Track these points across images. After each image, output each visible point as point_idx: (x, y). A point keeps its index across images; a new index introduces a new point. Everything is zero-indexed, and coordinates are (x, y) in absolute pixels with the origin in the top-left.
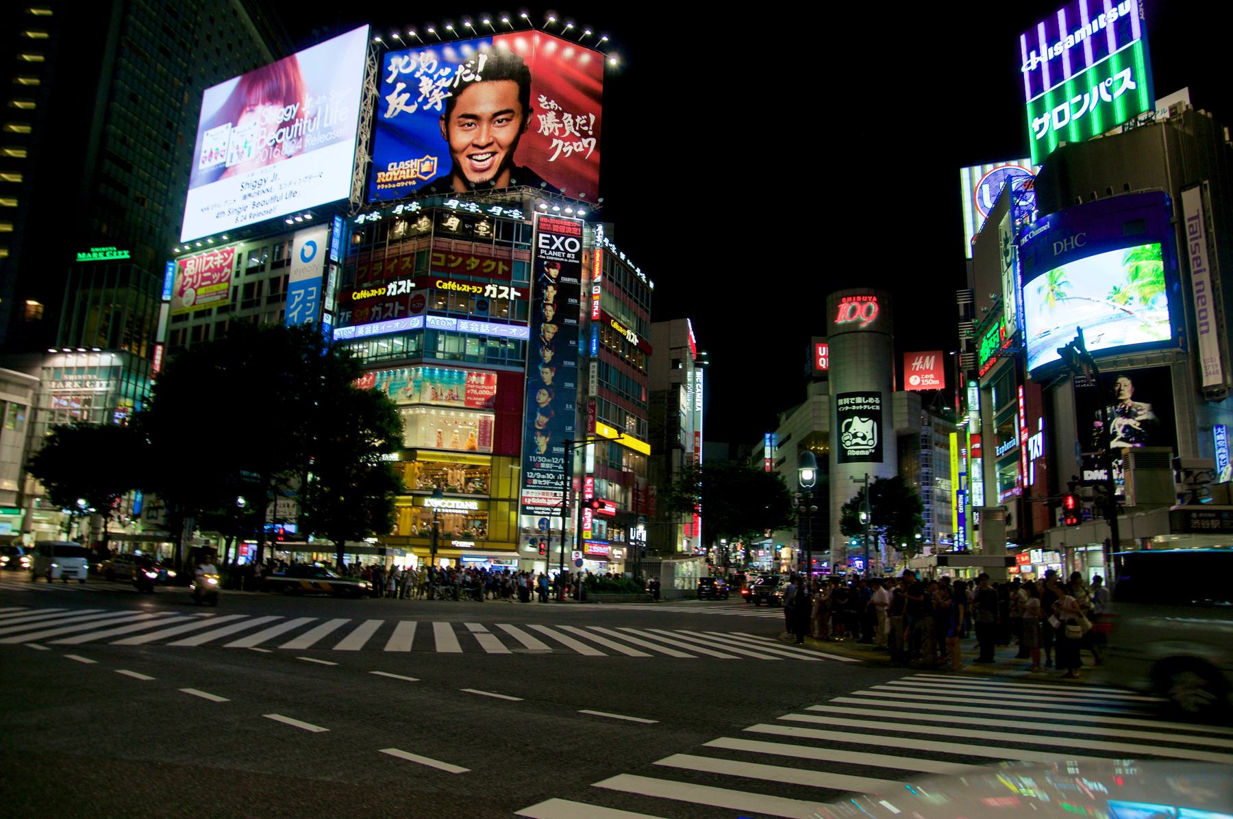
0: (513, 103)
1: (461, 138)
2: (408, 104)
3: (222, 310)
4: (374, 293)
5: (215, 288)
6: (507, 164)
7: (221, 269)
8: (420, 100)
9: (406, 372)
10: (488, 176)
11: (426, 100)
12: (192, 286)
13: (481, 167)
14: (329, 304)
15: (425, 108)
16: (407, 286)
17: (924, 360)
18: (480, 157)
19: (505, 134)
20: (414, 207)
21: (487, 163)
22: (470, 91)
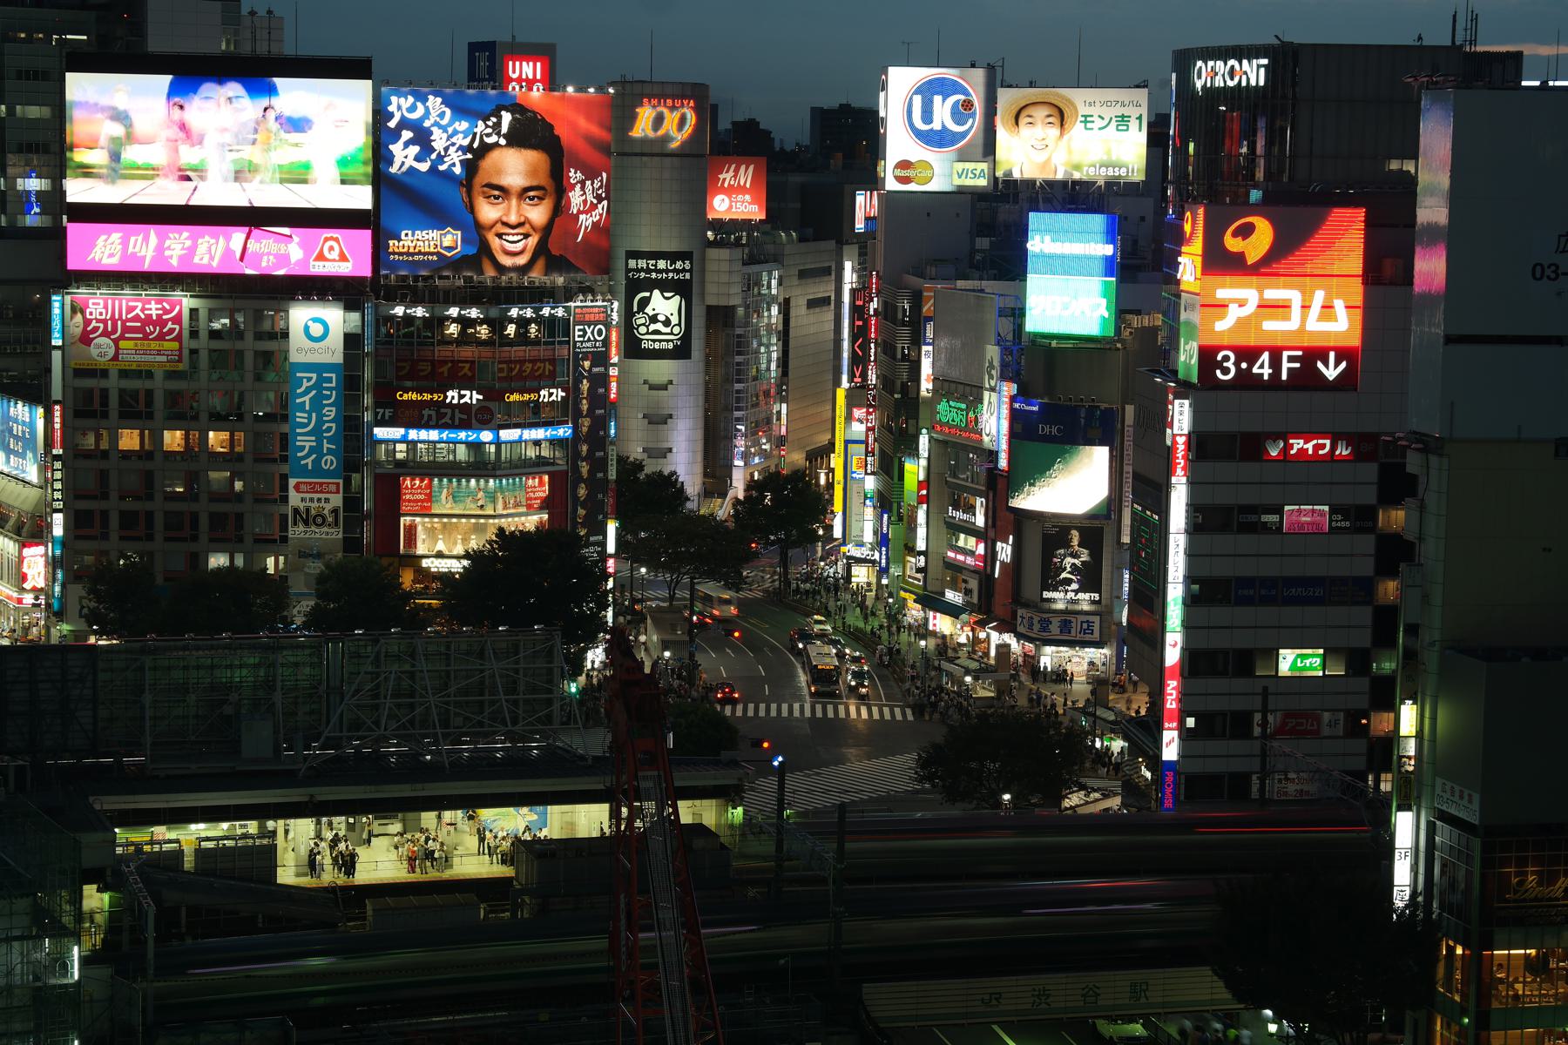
0: (543, 179)
1: (488, 212)
2: (418, 159)
3: (171, 375)
4: (427, 397)
5: (154, 345)
6: (541, 250)
7: (160, 322)
8: (434, 156)
9: (473, 481)
10: (522, 260)
11: (441, 158)
12: (105, 334)
13: (513, 250)
14: (368, 400)
15: (442, 168)
16: (472, 397)
17: (736, 171)
18: (510, 238)
19: (538, 214)
20: (474, 313)
21: (519, 246)
22: (495, 155)
